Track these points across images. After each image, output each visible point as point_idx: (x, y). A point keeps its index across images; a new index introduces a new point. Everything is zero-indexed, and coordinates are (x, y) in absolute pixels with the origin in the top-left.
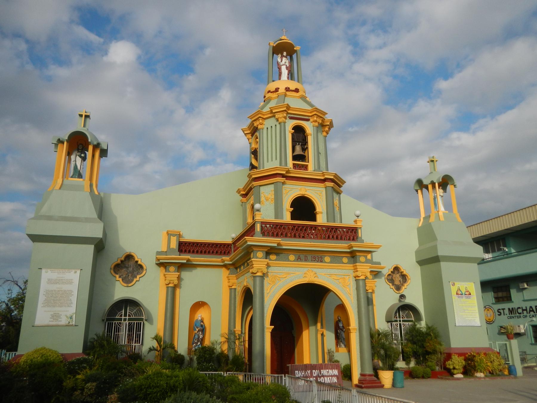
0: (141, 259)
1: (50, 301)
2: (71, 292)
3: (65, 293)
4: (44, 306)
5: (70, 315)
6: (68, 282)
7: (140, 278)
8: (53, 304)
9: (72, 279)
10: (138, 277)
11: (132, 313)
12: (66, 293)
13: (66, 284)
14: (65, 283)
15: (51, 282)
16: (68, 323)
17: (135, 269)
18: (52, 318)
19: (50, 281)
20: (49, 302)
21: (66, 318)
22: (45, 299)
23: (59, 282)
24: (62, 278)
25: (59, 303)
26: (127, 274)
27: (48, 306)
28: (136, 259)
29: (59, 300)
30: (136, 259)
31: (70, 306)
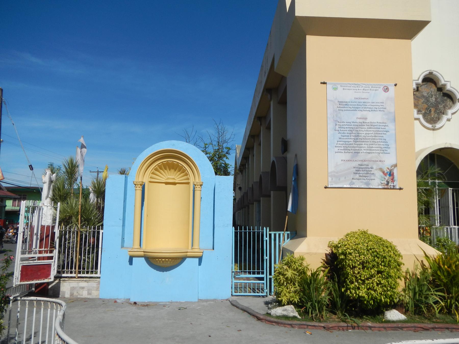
0: (450, 81)
1: (348, 142)
2: (385, 126)
3: (375, 128)
4: (340, 151)
5: (388, 169)
6: (376, 107)
8: (354, 147)
9: (382, 103)
10: (450, 112)
11: (444, 174)
12: (375, 127)
13: (372, 110)
14: (370, 109)
15: (345, 106)
16: (386, 183)
18: (357, 173)
20: (347, 143)
21: (382, 174)
22: (340, 138)
23: (360, 106)
24: (362, 101)
25: (366, 146)
27: (346, 151)
29: (365, 140)
30: (443, 82)
31: (386, 152)
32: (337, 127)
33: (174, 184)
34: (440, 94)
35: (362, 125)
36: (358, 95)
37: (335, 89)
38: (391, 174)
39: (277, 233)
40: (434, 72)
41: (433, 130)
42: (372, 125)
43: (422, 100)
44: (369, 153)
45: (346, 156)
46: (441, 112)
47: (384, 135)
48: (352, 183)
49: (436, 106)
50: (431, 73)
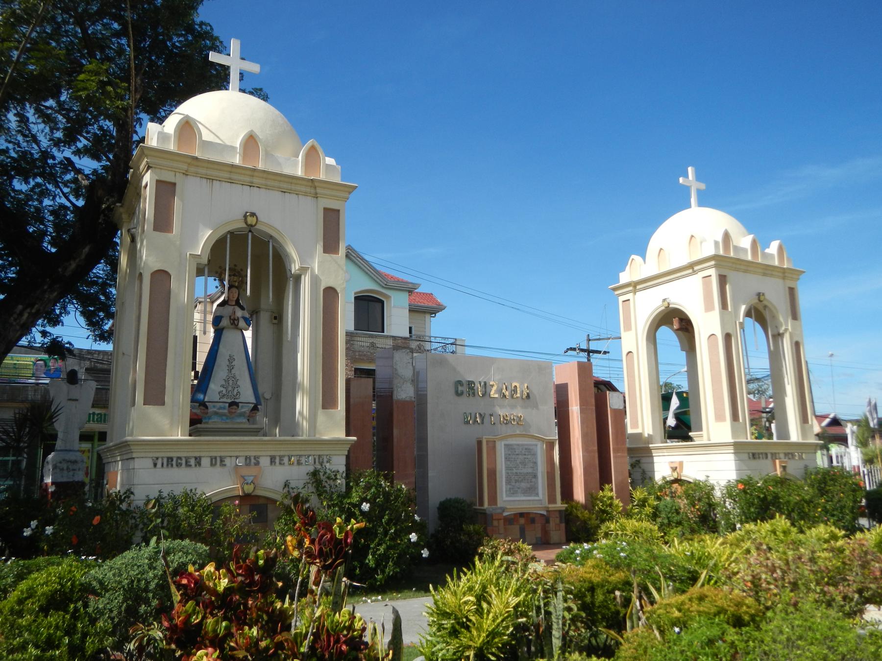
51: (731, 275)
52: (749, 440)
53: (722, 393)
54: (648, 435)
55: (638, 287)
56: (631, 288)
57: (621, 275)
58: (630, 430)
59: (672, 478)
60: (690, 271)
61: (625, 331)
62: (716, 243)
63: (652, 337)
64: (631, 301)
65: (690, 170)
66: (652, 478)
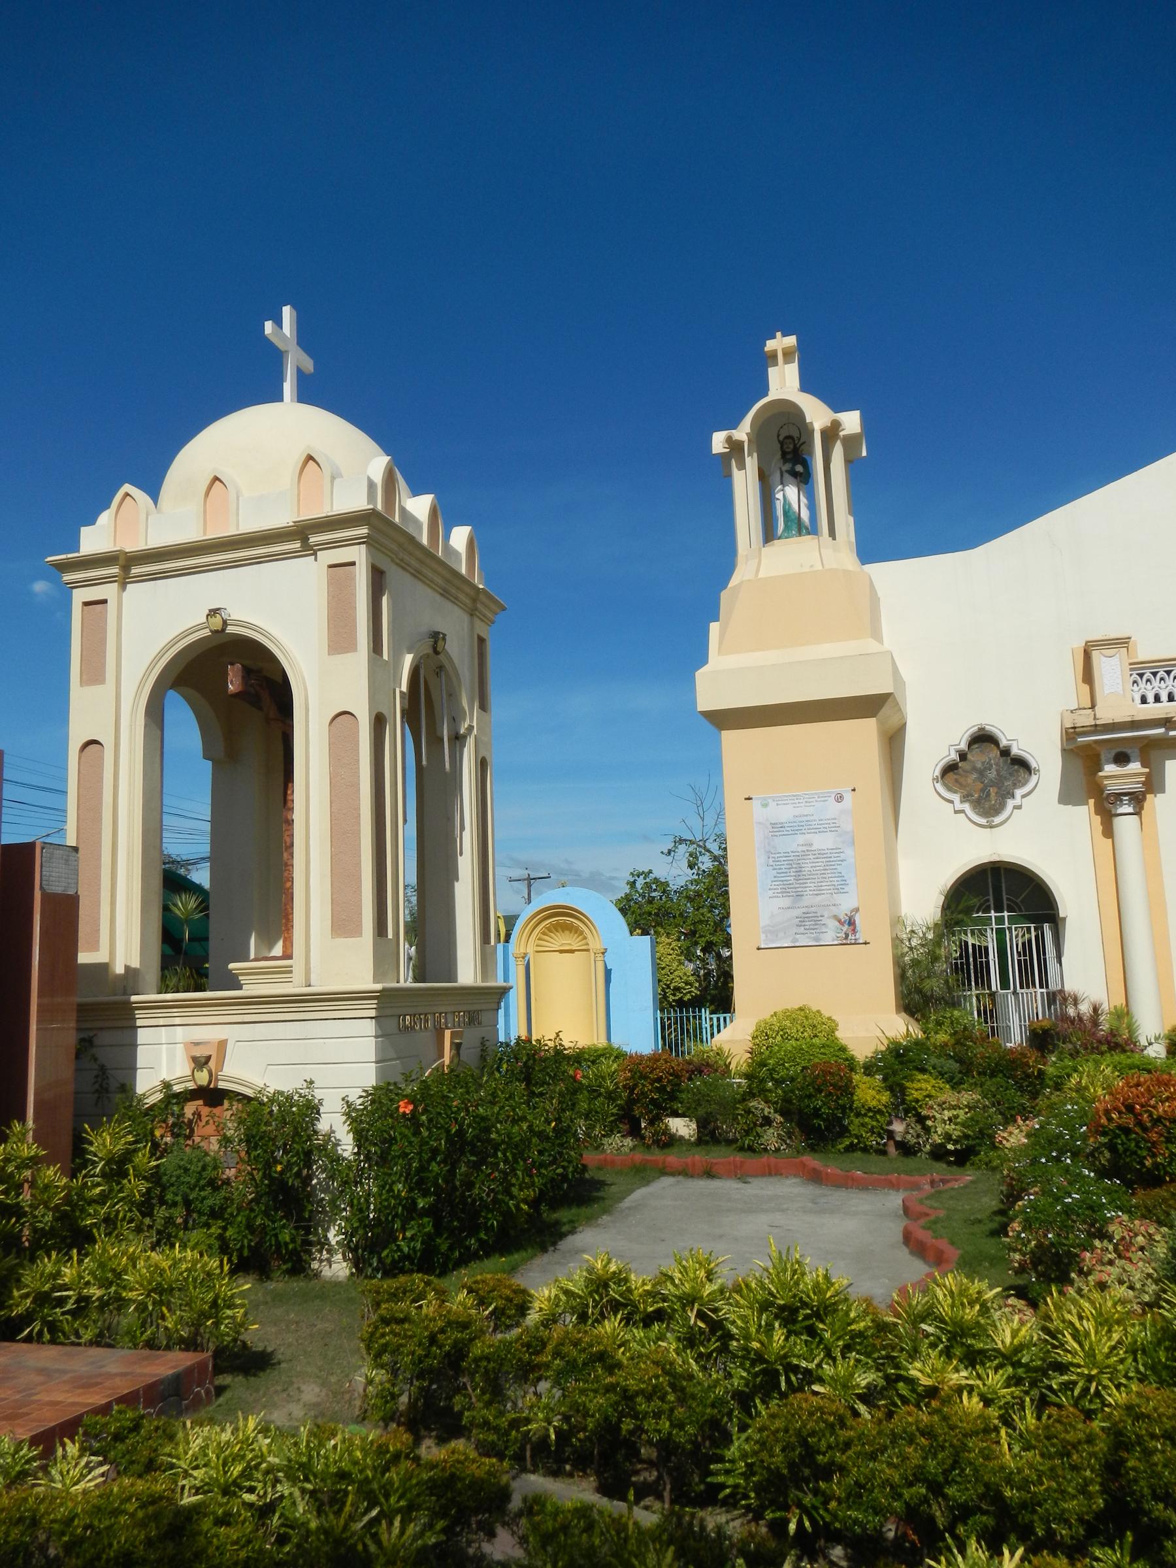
7: (1023, 796)
10: (1019, 793)
11: (1018, 901)
17: (1003, 773)
19: (777, 828)
24: (806, 819)
26: (982, 790)
28: (1004, 743)
32: (771, 860)
33: (572, 951)
34: (1006, 761)
35: (805, 854)
36: (798, 812)
37: (765, 805)
38: (851, 923)
39: (722, 1016)
40: (988, 728)
41: (991, 827)
42: (821, 854)
43: (975, 776)
44: (817, 895)
45: (785, 902)
46: (1008, 793)
47: (838, 867)
48: (796, 940)
49: (998, 783)
50: (982, 729)
51: (394, 575)
52: (402, 984)
53: (358, 865)
54: (127, 968)
55: (135, 571)
56: (115, 570)
57: (85, 531)
58: (84, 958)
59: (191, 1086)
60: (297, 545)
61: (83, 683)
62: (371, 485)
63: (155, 713)
64: (111, 606)
65: (287, 311)
66: (127, 1088)
